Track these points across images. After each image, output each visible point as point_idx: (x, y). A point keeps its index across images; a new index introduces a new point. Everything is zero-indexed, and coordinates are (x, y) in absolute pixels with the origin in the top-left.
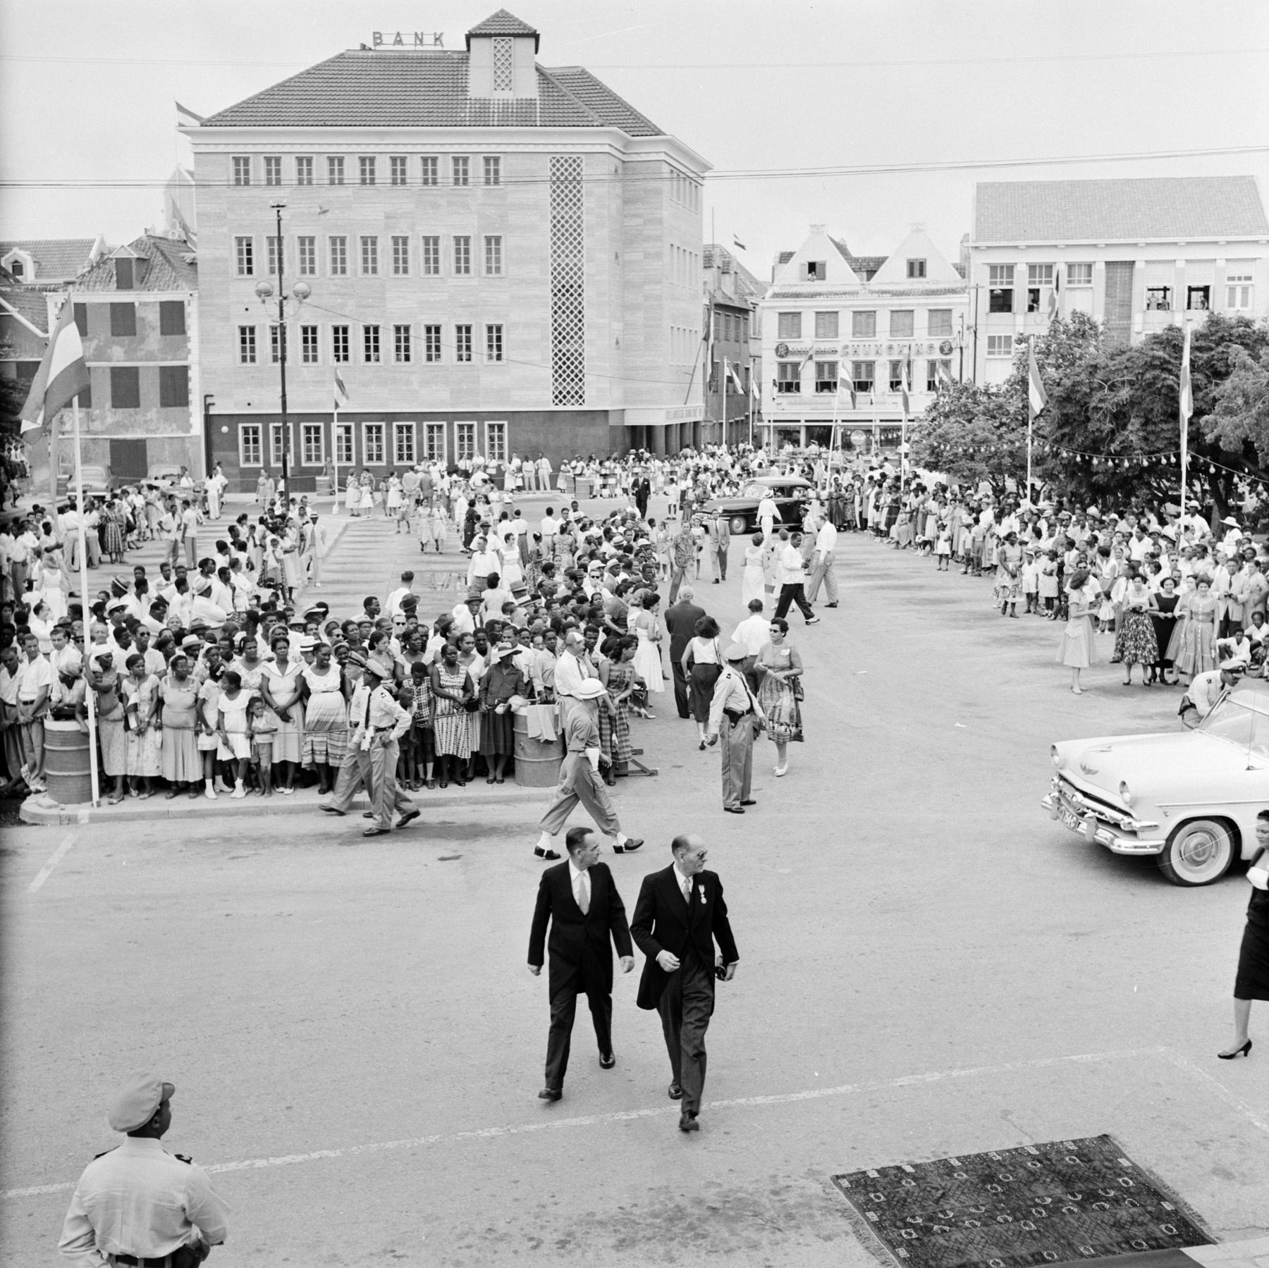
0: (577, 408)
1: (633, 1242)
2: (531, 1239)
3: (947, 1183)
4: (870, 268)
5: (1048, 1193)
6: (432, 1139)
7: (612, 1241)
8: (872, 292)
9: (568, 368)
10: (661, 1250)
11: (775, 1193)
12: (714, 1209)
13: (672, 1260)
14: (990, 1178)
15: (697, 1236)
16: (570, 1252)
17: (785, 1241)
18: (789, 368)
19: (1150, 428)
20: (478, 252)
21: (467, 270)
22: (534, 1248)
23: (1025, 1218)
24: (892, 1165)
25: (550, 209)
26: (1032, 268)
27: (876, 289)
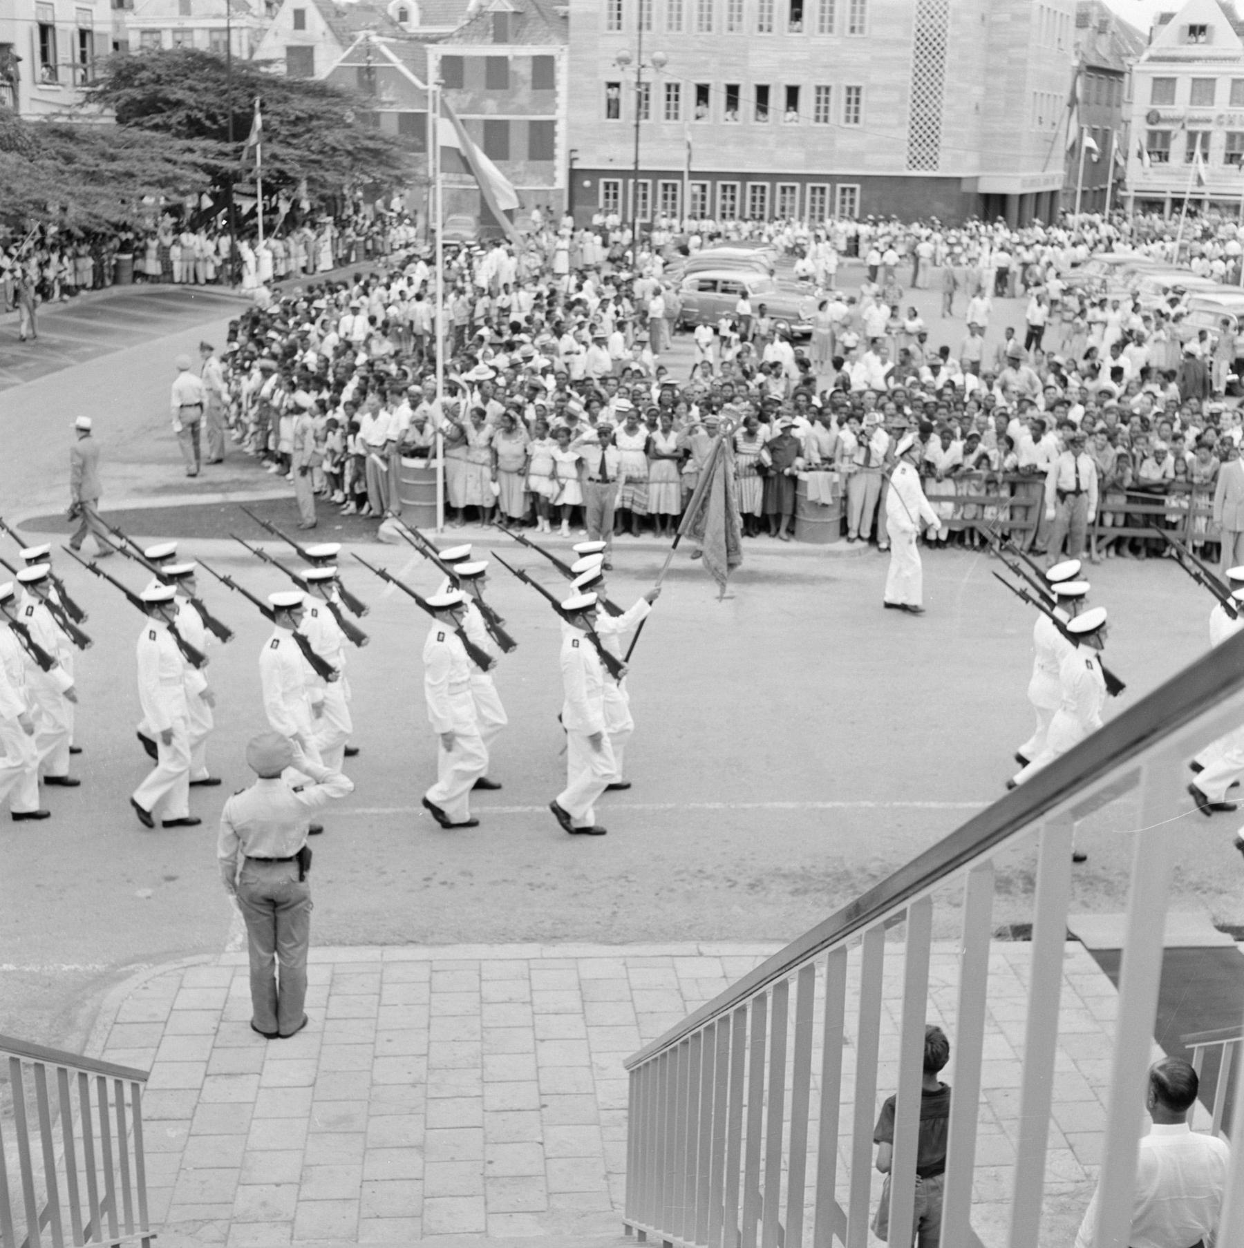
6: (669, 806)
7: (790, 888)
9: (925, 134)
18: (1159, 137)
21: (830, 30)
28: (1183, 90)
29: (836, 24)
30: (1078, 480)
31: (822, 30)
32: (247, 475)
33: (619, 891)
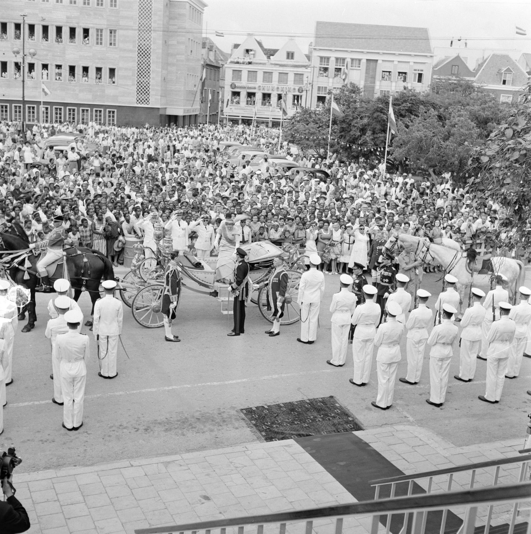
0: (146, 106)
1: (171, 430)
2: (135, 428)
4: (270, 53)
5: (313, 414)
6: (99, 395)
7: (164, 429)
8: (272, 64)
9: (143, 90)
10: (180, 432)
11: (220, 414)
12: (199, 419)
13: (184, 435)
14: (293, 410)
15: (193, 428)
16: (149, 433)
17: (222, 429)
19: (375, 136)
20: (106, 35)
21: (101, 44)
22: (136, 431)
23: (304, 423)
25: (138, 19)
26: (337, 59)
27: (273, 63)
28: (245, 75)
29: (103, 41)
31: (97, 43)
33: (85, 439)
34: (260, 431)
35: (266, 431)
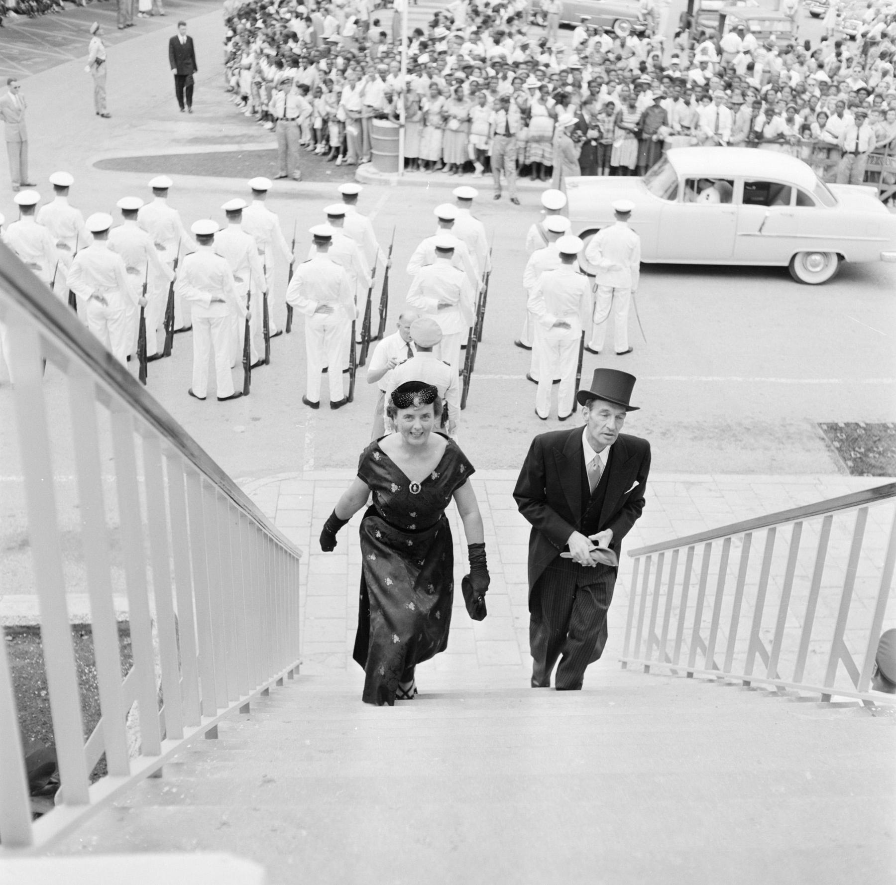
1: (702, 439)
3: (883, 434)
11: (783, 426)
12: (749, 429)
13: (721, 449)
15: (736, 440)
24: (853, 421)
30: (857, 144)
32: (253, 130)
34: (845, 459)
35: (855, 460)
